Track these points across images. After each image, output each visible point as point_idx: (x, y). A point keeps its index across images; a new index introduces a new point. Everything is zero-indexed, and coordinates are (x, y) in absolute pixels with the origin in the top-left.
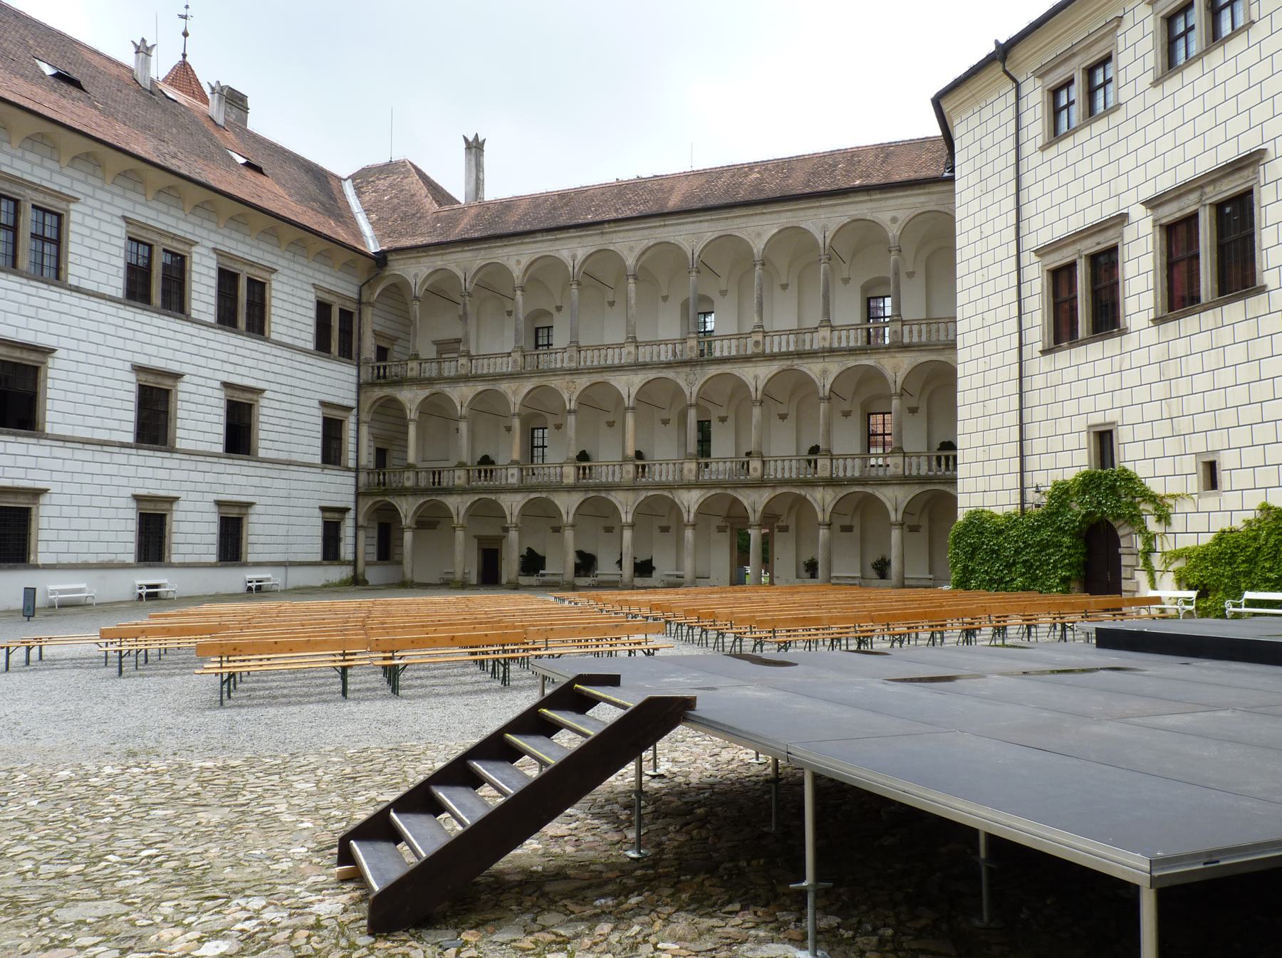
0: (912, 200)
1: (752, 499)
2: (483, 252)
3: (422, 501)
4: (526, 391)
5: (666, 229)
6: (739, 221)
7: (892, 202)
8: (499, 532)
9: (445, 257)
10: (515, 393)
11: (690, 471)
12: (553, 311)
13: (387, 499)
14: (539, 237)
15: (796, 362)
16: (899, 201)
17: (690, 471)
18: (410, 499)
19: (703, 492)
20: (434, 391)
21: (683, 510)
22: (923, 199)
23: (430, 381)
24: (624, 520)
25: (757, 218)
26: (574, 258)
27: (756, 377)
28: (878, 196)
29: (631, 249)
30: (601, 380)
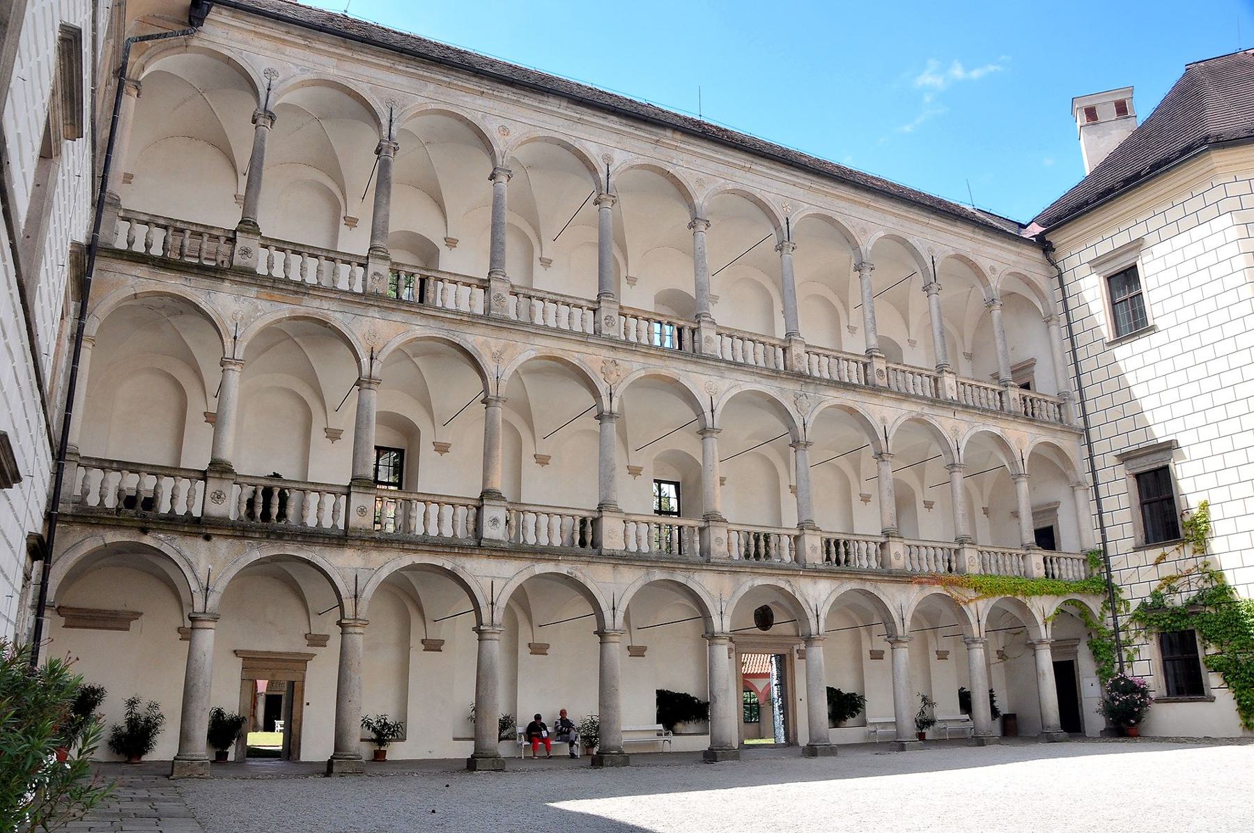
0: (1005, 255)
1: (897, 604)
2: (431, 87)
3: (256, 555)
4: (522, 359)
5: (749, 175)
6: (843, 204)
7: (989, 250)
8: (301, 646)
9: (349, 66)
10: (497, 357)
11: (814, 549)
12: (441, 245)
13: (148, 540)
14: (553, 104)
15: (926, 410)
16: (996, 252)
17: (814, 549)
18: (222, 546)
19: (835, 584)
20: (301, 311)
21: (810, 615)
22: (1013, 258)
23: (301, 289)
24: (717, 628)
25: (862, 209)
26: (608, 161)
27: (883, 420)
28: (980, 237)
29: (700, 182)
30: (664, 372)
